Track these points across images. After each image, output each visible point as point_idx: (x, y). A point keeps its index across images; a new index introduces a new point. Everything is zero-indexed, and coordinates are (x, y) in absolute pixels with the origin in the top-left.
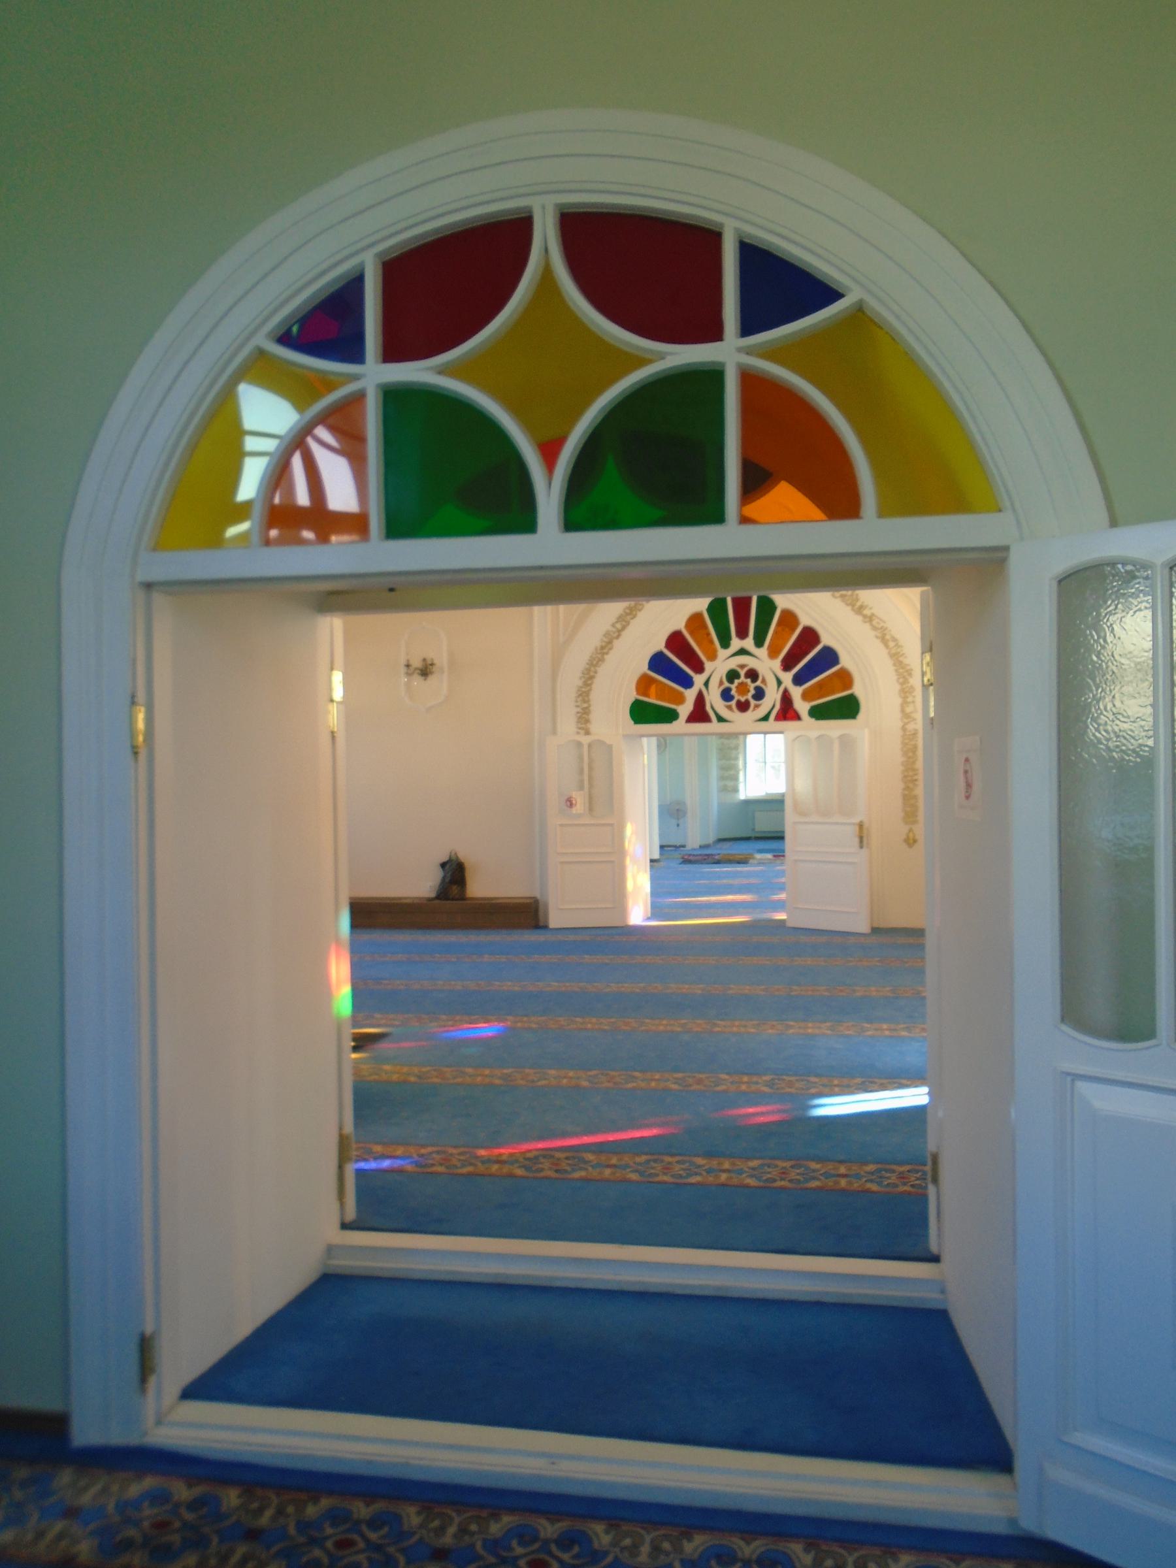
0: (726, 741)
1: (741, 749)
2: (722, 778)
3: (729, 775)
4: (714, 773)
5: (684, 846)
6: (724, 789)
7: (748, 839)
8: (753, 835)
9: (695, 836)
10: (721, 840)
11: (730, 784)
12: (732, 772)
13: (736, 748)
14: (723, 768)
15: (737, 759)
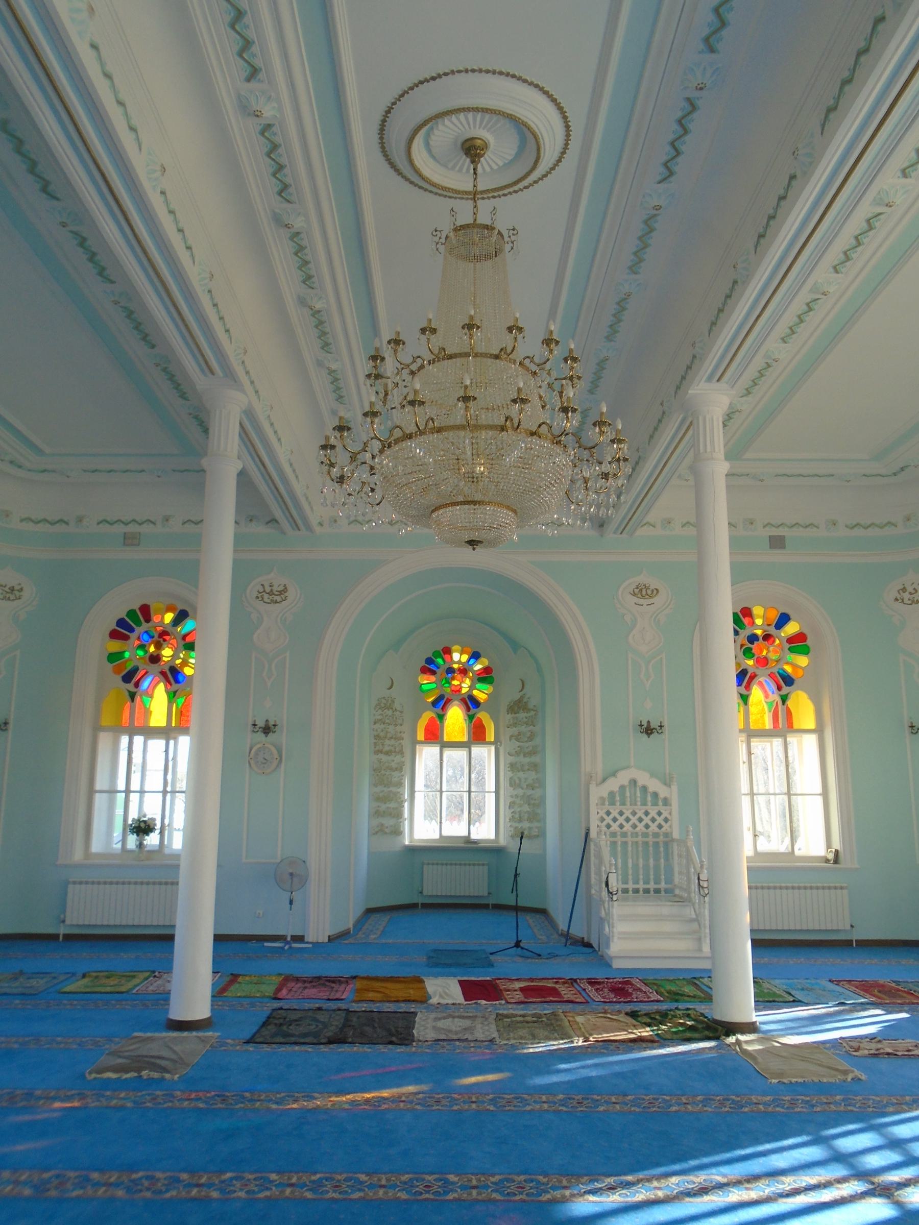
0: (384, 758)
1: (407, 768)
2: (377, 813)
3: (389, 808)
4: (364, 804)
5: (299, 939)
6: (379, 831)
7: (413, 906)
8: (420, 900)
9: (322, 915)
10: (370, 911)
11: (388, 822)
12: (392, 805)
13: (400, 769)
14: (377, 798)
15: (400, 784)
